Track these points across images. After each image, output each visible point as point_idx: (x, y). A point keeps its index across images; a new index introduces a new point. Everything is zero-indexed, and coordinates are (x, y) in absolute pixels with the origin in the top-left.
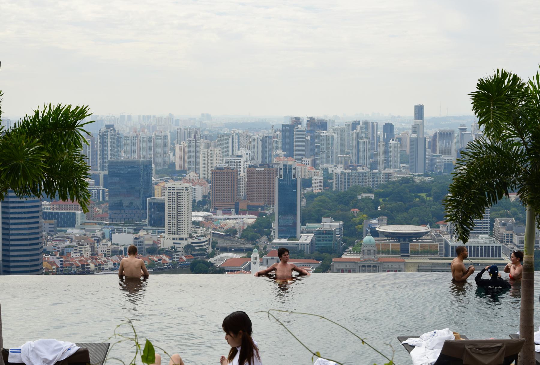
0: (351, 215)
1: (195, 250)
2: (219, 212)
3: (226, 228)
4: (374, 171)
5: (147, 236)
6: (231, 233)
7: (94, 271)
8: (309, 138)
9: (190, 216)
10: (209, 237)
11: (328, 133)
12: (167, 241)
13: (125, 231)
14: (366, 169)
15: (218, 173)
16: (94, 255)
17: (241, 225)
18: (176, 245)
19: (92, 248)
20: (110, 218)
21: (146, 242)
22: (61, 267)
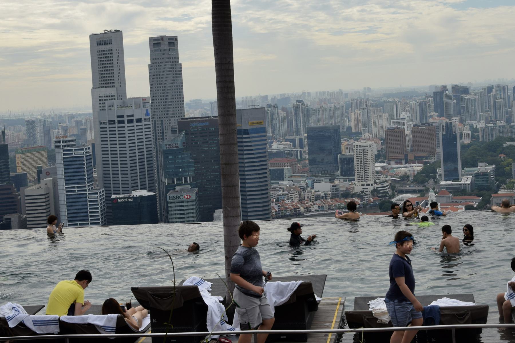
0: (500, 160)
1: (380, 193)
2: (392, 162)
3: (400, 175)
4: (512, 124)
5: (340, 183)
6: (405, 178)
7: (304, 213)
8: (455, 101)
9: (375, 167)
10: (390, 182)
11: (471, 96)
12: (357, 188)
13: (322, 181)
14: (503, 123)
15: (390, 132)
16: (301, 200)
17: (412, 172)
18: (365, 190)
19: (300, 195)
20: (310, 171)
21: (341, 189)
22: (279, 211)
